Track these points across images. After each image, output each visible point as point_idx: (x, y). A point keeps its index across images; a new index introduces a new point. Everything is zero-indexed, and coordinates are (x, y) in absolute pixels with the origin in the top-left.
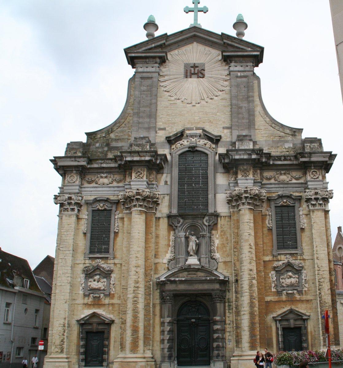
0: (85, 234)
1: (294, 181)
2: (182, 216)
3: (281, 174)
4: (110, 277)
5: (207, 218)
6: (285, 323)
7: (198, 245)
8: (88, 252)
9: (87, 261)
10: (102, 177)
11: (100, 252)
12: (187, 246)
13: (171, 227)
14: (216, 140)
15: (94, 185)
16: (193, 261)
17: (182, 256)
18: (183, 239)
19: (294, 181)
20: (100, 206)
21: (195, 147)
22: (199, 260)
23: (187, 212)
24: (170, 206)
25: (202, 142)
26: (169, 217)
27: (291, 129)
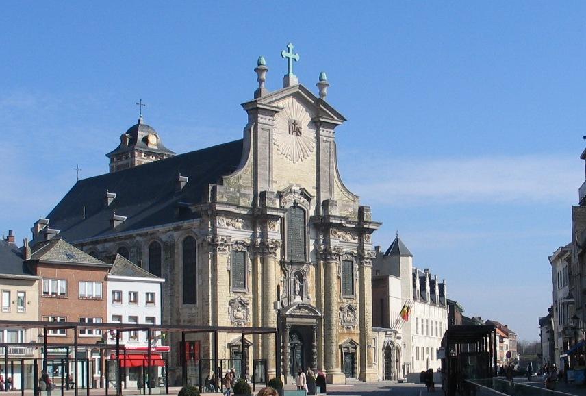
0: (229, 271)
1: (353, 241)
2: (291, 263)
3: (346, 234)
4: (247, 309)
5: (305, 266)
6: (346, 349)
7: (301, 287)
8: (231, 287)
9: (232, 295)
10: (237, 221)
11: (238, 287)
12: (295, 288)
13: (284, 271)
14: (308, 198)
15: (231, 227)
16: (298, 299)
17: (292, 295)
18: (292, 282)
19: (353, 241)
20: (241, 248)
21: (298, 204)
22: (302, 299)
23: (293, 259)
24: (282, 254)
25: (303, 199)
26: (282, 263)
27: (353, 195)
